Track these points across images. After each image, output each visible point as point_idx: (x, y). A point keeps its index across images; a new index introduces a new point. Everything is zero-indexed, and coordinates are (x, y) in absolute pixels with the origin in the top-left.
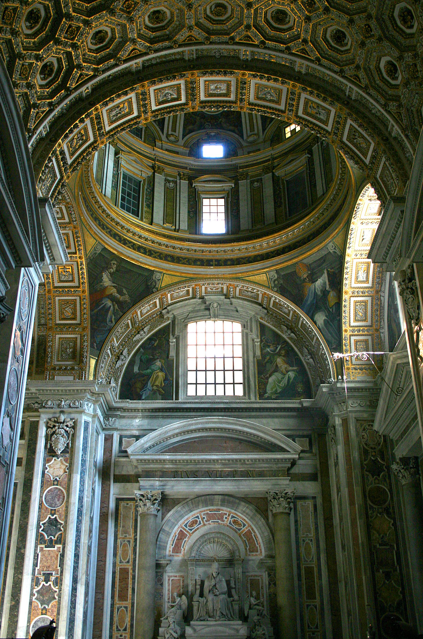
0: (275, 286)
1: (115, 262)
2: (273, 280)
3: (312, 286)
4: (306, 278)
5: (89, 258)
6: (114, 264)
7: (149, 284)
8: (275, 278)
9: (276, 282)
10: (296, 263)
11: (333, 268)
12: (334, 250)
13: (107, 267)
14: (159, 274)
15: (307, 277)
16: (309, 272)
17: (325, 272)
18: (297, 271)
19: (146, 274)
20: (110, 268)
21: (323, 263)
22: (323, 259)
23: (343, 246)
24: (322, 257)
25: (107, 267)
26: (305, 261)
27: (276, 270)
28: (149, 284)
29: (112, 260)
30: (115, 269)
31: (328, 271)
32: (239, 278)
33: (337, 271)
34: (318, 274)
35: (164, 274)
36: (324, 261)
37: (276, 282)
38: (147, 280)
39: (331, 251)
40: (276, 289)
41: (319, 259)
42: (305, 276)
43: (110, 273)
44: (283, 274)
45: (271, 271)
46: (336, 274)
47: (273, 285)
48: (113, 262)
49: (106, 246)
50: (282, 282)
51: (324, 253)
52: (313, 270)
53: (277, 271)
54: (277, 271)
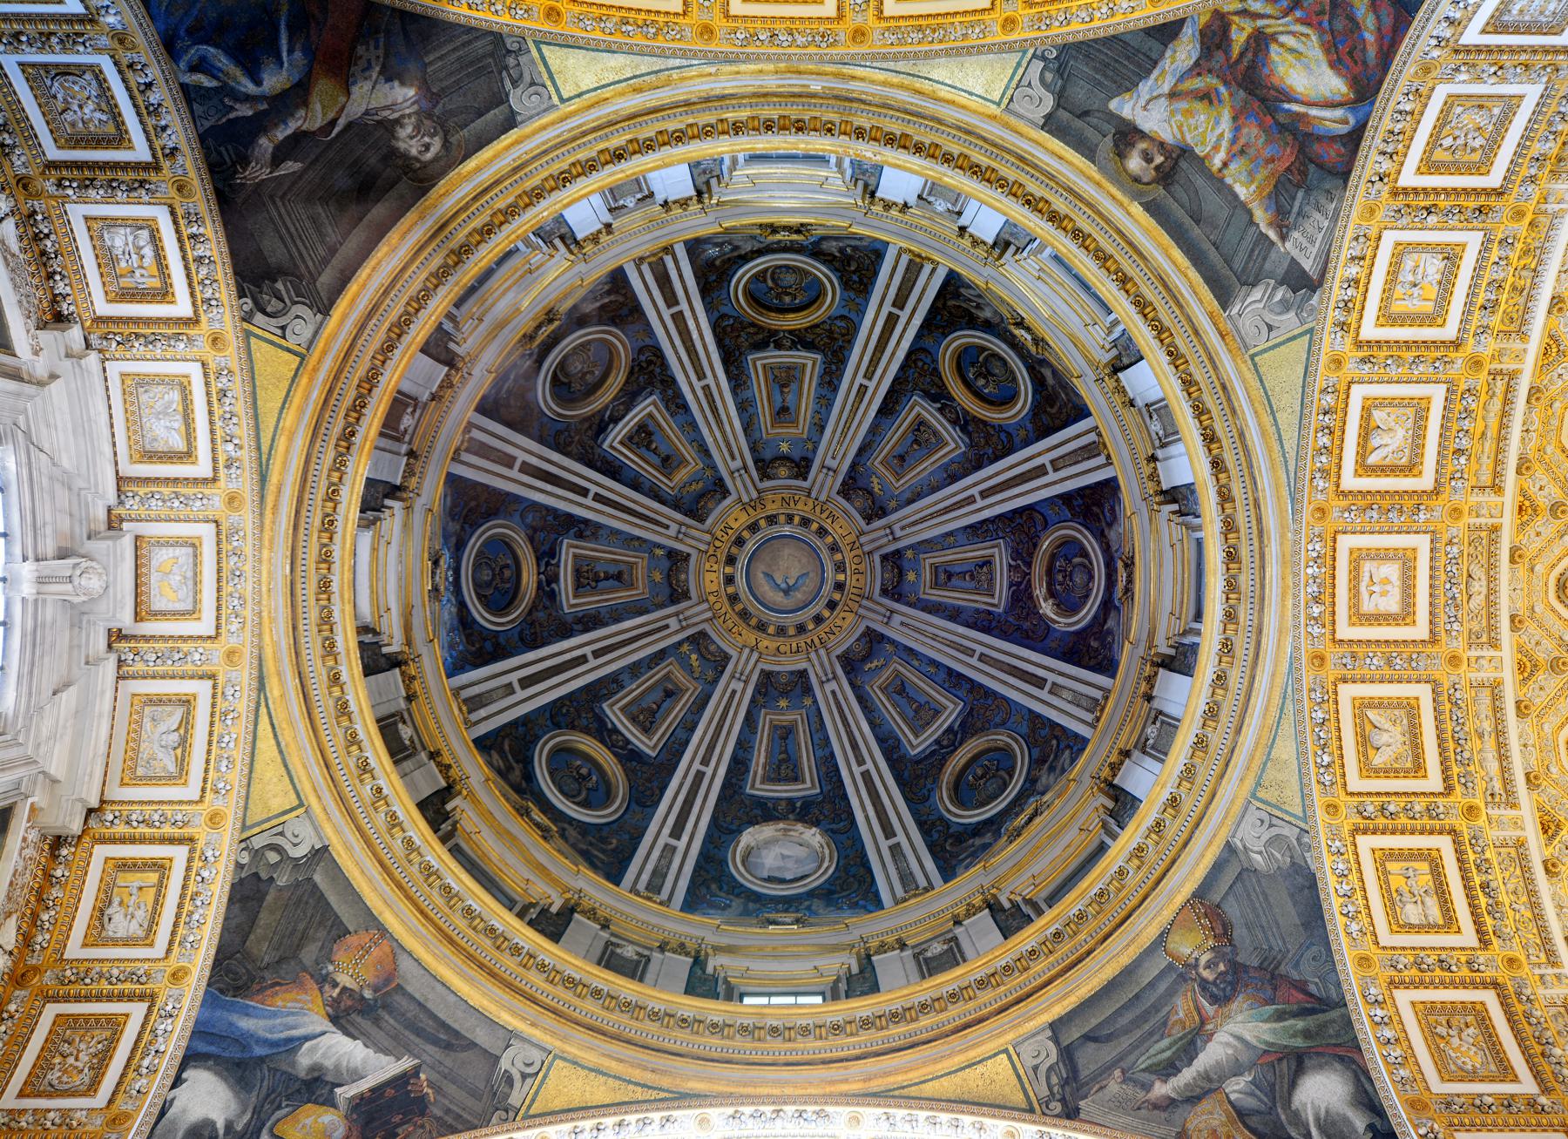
0: (257, 854)
1: (429, 156)
2: (279, 840)
3: (315, 1021)
4: (335, 985)
5: (521, 51)
6: (427, 147)
7: (280, 285)
8: (288, 847)
9: (273, 857)
10: (383, 931)
11: (438, 1090)
12: (517, 1077)
13: (434, 116)
14: (307, 333)
15: (345, 989)
16: (368, 994)
17: (406, 1063)
18: (351, 940)
19: (326, 279)
20: (417, 128)
21: (435, 1042)
22: (451, 1040)
23: (558, 1104)
24: (457, 1034)
25: (430, 116)
26: (405, 964)
27: (325, 848)
28: (280, 285)
29: (446, 144)
30: (402, 146)
31: (415, 1071)
32: (261, 687)
33: (437, 1112)
34: (373, 1030)
35: (303, 357)
36: (448, 1047)
37: (273, 857)
38: (300, 278)
39: (504, 1064)
40: (245, 858)
41: (443, 1025)
42: (344, 980)
43: (398, 122)
44: (317, 878)
45: (317, 829)
46: (422, 1114)
47: (257, 843)
48: (436, 145)
49: (513, 135)
50: (282, 880)
51: (482, 1037)
52: (384, 1007)
53: (321, 854)
54: (321, 854)
